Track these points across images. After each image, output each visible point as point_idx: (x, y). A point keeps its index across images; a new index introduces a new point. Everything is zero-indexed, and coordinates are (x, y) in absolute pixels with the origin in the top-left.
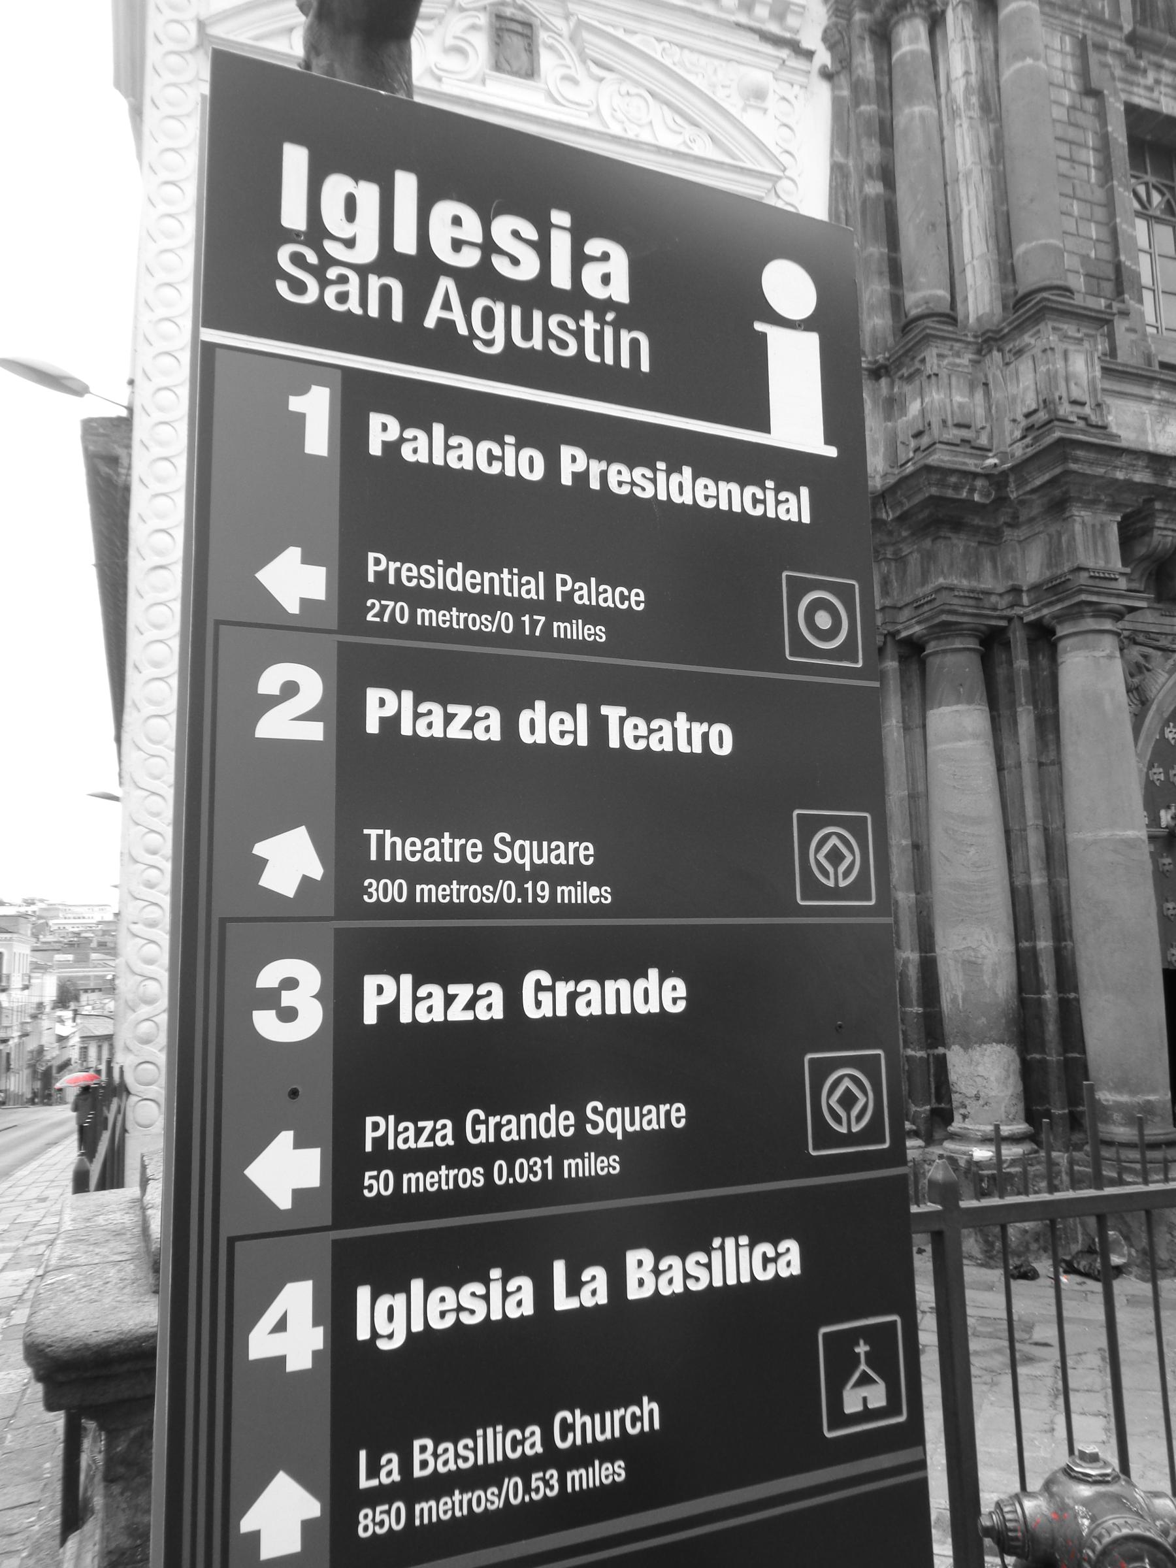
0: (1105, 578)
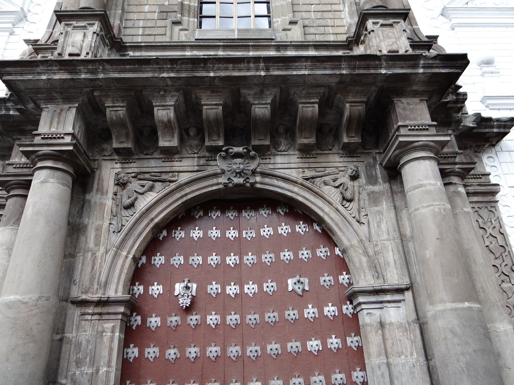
0: (55, 138)
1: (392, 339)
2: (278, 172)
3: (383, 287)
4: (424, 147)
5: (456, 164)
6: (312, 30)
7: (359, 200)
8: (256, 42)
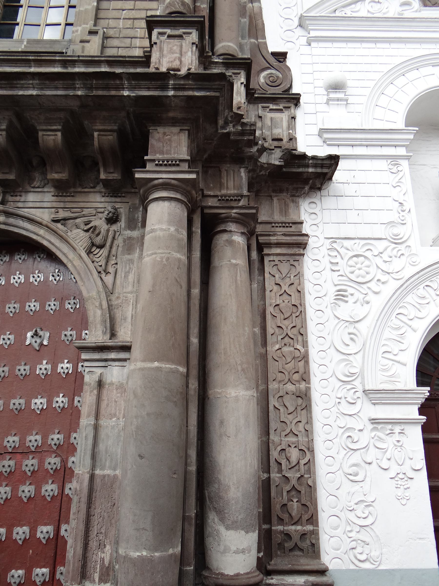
1: (108, 400)
2: (22, 212)
3: (105, 344)
4: (166, 186)
5: (233, 208)
6: (115, 43)
7: (111, 247)
8: (38, 56)
